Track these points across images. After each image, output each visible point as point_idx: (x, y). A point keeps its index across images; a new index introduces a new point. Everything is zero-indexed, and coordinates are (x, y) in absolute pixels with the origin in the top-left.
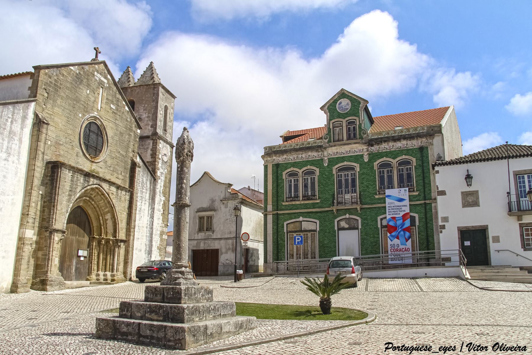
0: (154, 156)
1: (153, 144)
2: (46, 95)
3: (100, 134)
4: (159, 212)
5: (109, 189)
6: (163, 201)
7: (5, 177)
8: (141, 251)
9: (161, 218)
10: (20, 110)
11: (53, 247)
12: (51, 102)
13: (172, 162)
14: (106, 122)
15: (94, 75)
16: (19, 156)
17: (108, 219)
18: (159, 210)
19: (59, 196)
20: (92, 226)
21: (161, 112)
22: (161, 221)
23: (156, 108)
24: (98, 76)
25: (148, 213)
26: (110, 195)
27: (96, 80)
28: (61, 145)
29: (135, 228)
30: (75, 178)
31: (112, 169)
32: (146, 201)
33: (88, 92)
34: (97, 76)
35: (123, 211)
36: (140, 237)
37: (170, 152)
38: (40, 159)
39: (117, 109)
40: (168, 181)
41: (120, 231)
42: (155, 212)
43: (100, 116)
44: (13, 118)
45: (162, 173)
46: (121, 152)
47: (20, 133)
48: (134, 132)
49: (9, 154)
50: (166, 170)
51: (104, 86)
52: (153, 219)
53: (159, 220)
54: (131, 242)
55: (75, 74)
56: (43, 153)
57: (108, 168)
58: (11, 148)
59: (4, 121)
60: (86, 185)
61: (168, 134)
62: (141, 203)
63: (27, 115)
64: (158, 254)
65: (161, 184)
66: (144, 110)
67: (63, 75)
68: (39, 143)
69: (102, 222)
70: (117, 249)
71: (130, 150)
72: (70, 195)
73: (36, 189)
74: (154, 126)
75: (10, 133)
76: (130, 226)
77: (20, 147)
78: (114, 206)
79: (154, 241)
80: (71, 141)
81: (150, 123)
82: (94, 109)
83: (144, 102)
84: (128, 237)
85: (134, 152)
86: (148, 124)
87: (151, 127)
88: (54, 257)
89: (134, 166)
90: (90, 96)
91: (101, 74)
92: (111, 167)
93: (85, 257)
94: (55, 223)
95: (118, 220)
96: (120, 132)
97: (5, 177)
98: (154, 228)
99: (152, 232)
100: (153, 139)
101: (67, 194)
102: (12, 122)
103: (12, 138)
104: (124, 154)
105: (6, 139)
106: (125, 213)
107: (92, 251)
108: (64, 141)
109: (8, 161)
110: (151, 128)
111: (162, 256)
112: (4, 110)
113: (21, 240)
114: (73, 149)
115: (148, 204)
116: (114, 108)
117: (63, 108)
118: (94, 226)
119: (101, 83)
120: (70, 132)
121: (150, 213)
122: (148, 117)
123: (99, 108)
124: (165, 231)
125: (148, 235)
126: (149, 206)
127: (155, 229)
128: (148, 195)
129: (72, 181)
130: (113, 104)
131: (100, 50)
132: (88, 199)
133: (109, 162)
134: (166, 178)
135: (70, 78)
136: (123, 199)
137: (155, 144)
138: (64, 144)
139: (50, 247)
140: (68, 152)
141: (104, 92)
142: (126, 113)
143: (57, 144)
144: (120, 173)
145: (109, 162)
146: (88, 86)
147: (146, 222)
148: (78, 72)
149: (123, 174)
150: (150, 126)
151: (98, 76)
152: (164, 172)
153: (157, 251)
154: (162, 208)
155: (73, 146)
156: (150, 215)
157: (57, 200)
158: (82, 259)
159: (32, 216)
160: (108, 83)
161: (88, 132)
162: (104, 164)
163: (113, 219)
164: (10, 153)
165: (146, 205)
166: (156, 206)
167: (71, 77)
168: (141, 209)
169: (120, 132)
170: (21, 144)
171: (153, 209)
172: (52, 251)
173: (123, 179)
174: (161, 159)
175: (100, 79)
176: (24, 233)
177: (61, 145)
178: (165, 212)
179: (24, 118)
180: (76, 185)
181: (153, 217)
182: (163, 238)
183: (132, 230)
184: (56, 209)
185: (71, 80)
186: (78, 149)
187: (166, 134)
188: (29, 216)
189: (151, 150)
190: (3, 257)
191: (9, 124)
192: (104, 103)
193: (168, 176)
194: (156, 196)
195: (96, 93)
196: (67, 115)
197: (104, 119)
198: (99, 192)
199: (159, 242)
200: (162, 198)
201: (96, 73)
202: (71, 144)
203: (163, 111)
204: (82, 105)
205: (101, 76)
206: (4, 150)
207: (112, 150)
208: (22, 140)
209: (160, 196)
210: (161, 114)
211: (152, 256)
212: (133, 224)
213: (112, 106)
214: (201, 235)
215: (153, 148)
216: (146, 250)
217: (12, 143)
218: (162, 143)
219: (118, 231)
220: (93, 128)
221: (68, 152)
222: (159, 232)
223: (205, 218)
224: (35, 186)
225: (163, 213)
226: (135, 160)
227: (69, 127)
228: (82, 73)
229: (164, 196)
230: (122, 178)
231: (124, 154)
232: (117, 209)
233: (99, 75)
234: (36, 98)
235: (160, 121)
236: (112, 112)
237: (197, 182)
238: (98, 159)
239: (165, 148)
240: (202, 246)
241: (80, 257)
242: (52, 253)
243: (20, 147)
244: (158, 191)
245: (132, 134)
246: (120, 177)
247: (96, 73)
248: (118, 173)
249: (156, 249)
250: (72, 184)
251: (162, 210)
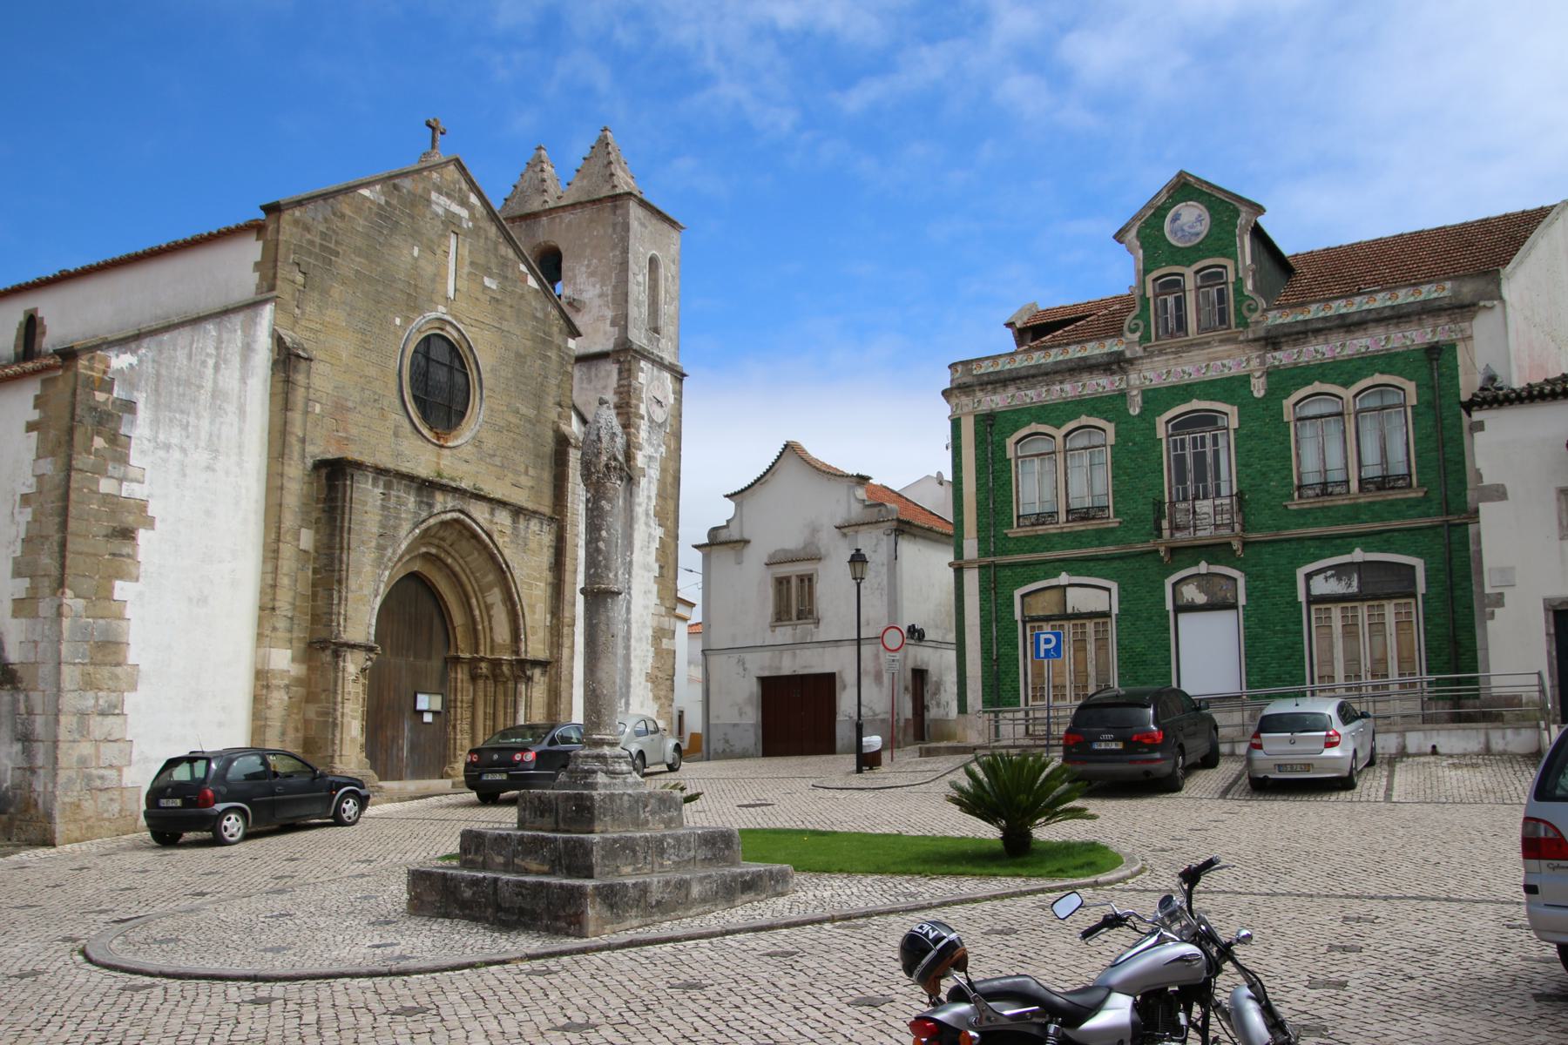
0: (624, 411)
1: (620, 372)
2: (300, 278)
3: (457, 364)
4: (646, 574)
5: (491, 522)
6: (658, 541)
7: (208, 513)
9: (655, 588)
10: (235, 331)
11: (343, 692)
12: (316, 295)
13: (680, 421)
14: (473, 329)
15: (429, 202)
16: (240, 454)
17: (493, 604)
18: (647, 568)
19: (352, 555)
20: (450, 627)
21: (640, 278)
22: (654, 599)
23: (624, 266)
24: (442, 203)
26: (495, 537)
27: (437, 215)
28: (348, 410)
29: (574, 625)
30: (393, 500)
31: (498, 461)
33: (416, 252)
34: (437, 204)
35: (535, 579)
37: (674, 393)
38: (296, 455)
39: (503, 290)
40: (670, 479)
41: (530, 637)
42: (634, 573)
43: (455, 317)
44: (218, 355)
45: (650, 458)
46: (523, 410)
47: (240, 391)
48: (559, 348)
49: (215, 451)
50: (663, 449)
51: (459, 226)
53: (649, 595)
54: (565, 663)
55: (375, 209)
56: (303, 441)
57: (488, 460)
58: (219, 437)
59: (198, 367)
60: (424, 515)
61: (663, 341)
63: (255, 342)
64: (651, 695)
65: (649, 489)
66: (592, 274)
67: (343, 216)
68: (289, 414)
69: (477, 612)
70: (524, 686)
71: (550, 401)
72: (381, 548)
73: (288, 538)
74: (622, 321)
75: (213, 396)
76: (558, 619)
77: (241, 431)
78: (508, 566)
79: (636, 657)
80: (377, 397)
81: (609, 314)
82: (435, 299)
83: (588, 251)
84: (555, 651)
85: (561, 406)
86: (602, 316)
87: (613, 324)
88: (349, 719)
89: (562, 446)
90: (422, 263)
91: (448, 195)
92: (494, 456)
93: (435, 713)
94: (345, 627)
95: (522, 606)
96: (518, 355)
97: (208, 513)
98: (633, 620)
100: (618, 362)
101: (373, 544)
102: (217, 368)
103: (220, 408)
104: (532, 413)
105: (205, 414)
106: (542, 585)
107: (456, 695)
108: (358, 399)
109: (214, 470)
110: (612, 329)
111: (663, 700)
112: (196, 338)
113: (262, 677)
114: (383, 417)
116: (494, 287)
117: (348, 309)
118: (455, 625)
119: (451, 222)
120: (372, 371)
122: (601, 295)
123: (451, 294)
124: (666, 627)
127: (637, 622)
129: (384, 507)
130: (490, 276)
131: (441, 127)
132: (433, 551)
133: (490, 442)
134: (663, 470)
135: (361, 222)
136: (533, 545)
137: (626, 373)
138: (359, 408)
139: (335, 692)
140: (369, 428)
141: (463, 245)
142: (530, 297)
143: (340, 409)
144: (523, 470)
145: (490, 442)
146: (416, 235)
148: (383, 202)
149: (531, 472)
150: (608, 322)
151: (441, 203)
152: (658, 456)
153: (646, 687)
154: (657, 560)
155: (382, 409)
157: (348, 565)
158: (428, 718)
159: (285, 613)
160: (473, 217)
161: (423, 363)
162: (475, 450)
163: (508, 603)
164: (217, 451)
167: (366, 220)
169: (518, 355)
170: (244, 422)
172: (343, 703)
173: (533, 487)
174: (646, 418)
175: (447, 211)
176: (266, 659)
177: (348, 410)
178: (665, 571)
179: (248, 349)
180: (396, 518)
181: (629, 588)
182: (664, 646)
183: (566, 630)
184: (347, 587)
185: (364, 227)
186: (397, 417)
187: (658, 340)
188: (278, 612)
189: (616, 393)
190: (220, 724)
191: (209, 371)
192: (465, 276)
193: (671, 465)
194: (636, 526)
195: (439, 252)
196: (360, 325)
197: (467, 321)
198: (464, 532)
199: (650, 660)
200: (653, 532)
201: (434, 196)
202: (376, 405)
203: (644, 275)
204: (402, 291)
205: (449, 202)
206: (202, 444)
207: (496, 407)
208: (245, 412)
209: (647, 524)
210: (638, 284)
211: (631, 701)
212: (567, 614)
213: (487, 281)
214: (785, 634)
215: (619, 386)
217: (222, 423)
218: (645, 368)
219: (522, 637)
220: (439, 353)
221: (369, 428)
222: (649, 632)
223: (794, 582)
224: (288, 531)
225: (661, 575)
226: (564, 428)
227: (367, 358)
228: (394, 202)
229: (660, 525)
230: (530, 484)
231: (532, 413)
232: (517, 573)
233: (443, 200)
234: (275, 293)
235: (638, 305)
236: (488, 298)
237: (765, 474)
238: (456, 438)
239: (656, 383)
240: (789, 665)
241: (422, 712)
242: (343, 708)
243: (241, 431)
244: (639, 511)
245: (553, 354)
246: (524, 480)
247: (434, 196)
248: (516, 472)
249: (643, 679)
250: (386, 517)
251: (656, 567)
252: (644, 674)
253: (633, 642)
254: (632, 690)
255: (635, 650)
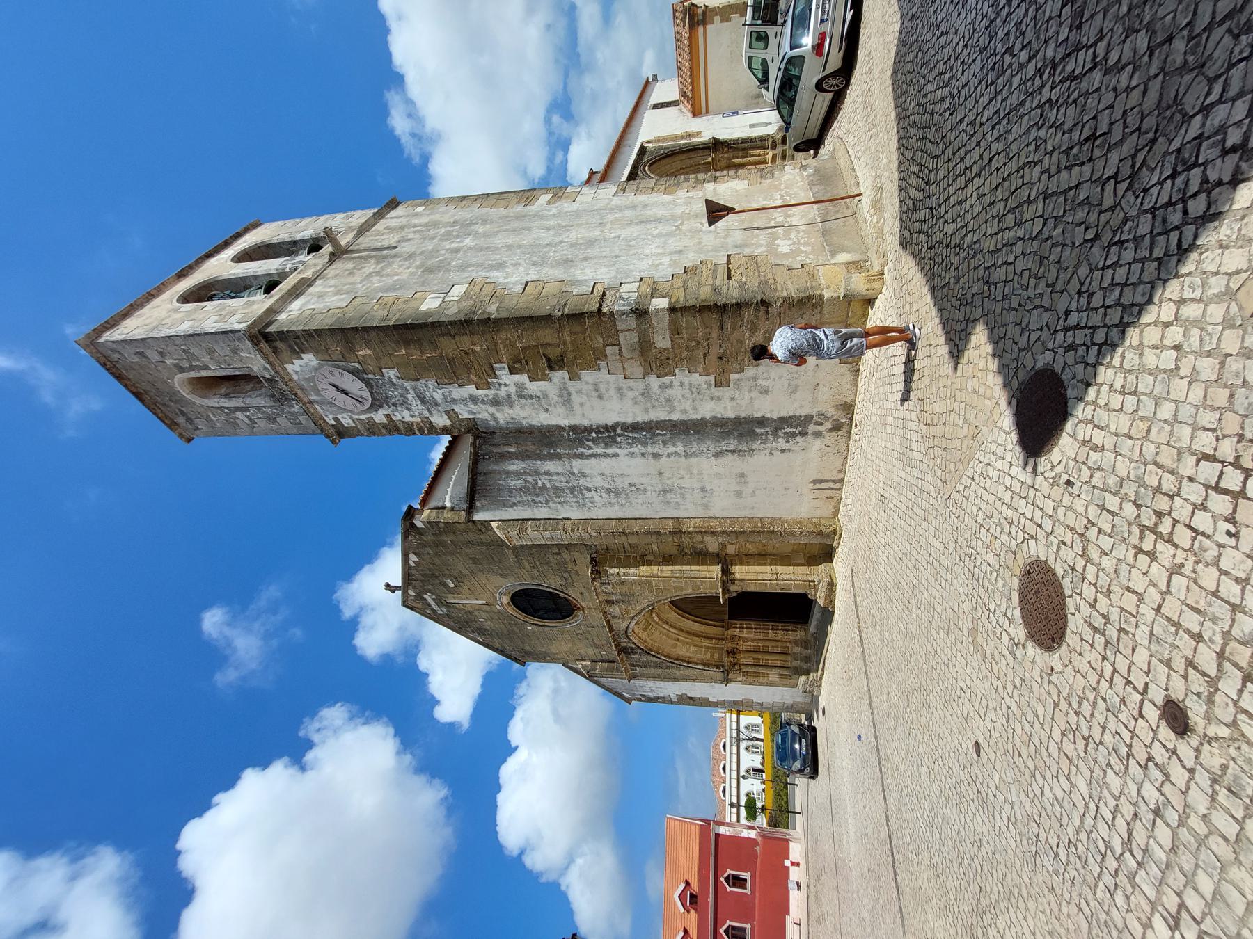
4: (576, 399)
8: (742, 475)
18: (566, 398)
25: (608, 456)
32: (573, 474)
36: (698, 485)
42: (585, 422)
52: (614, 427)
53: (602, 387)
62: (589, 490)
79: (695, 409)
99: (661, 425)
115: (577, 464)
121: (599, 450)
125: (680, 448)
126: (581, 456)
128: (550, 466)
147: (640, 460)
153: (738, 385)
156: (607, 446)
165: (587, 471)
166: (557, 418)
168: (609, 491)
171: (581, 435)
199: (696, 378)
216: (739, 452)
222: (654, 381)
249: (726, 392)
252: (717, 392)
253: (676, 416)
254: (743, 415)
255: (684, 411)
